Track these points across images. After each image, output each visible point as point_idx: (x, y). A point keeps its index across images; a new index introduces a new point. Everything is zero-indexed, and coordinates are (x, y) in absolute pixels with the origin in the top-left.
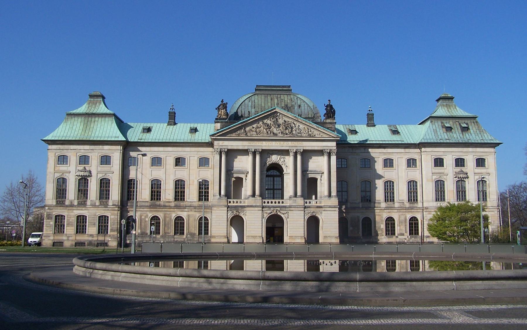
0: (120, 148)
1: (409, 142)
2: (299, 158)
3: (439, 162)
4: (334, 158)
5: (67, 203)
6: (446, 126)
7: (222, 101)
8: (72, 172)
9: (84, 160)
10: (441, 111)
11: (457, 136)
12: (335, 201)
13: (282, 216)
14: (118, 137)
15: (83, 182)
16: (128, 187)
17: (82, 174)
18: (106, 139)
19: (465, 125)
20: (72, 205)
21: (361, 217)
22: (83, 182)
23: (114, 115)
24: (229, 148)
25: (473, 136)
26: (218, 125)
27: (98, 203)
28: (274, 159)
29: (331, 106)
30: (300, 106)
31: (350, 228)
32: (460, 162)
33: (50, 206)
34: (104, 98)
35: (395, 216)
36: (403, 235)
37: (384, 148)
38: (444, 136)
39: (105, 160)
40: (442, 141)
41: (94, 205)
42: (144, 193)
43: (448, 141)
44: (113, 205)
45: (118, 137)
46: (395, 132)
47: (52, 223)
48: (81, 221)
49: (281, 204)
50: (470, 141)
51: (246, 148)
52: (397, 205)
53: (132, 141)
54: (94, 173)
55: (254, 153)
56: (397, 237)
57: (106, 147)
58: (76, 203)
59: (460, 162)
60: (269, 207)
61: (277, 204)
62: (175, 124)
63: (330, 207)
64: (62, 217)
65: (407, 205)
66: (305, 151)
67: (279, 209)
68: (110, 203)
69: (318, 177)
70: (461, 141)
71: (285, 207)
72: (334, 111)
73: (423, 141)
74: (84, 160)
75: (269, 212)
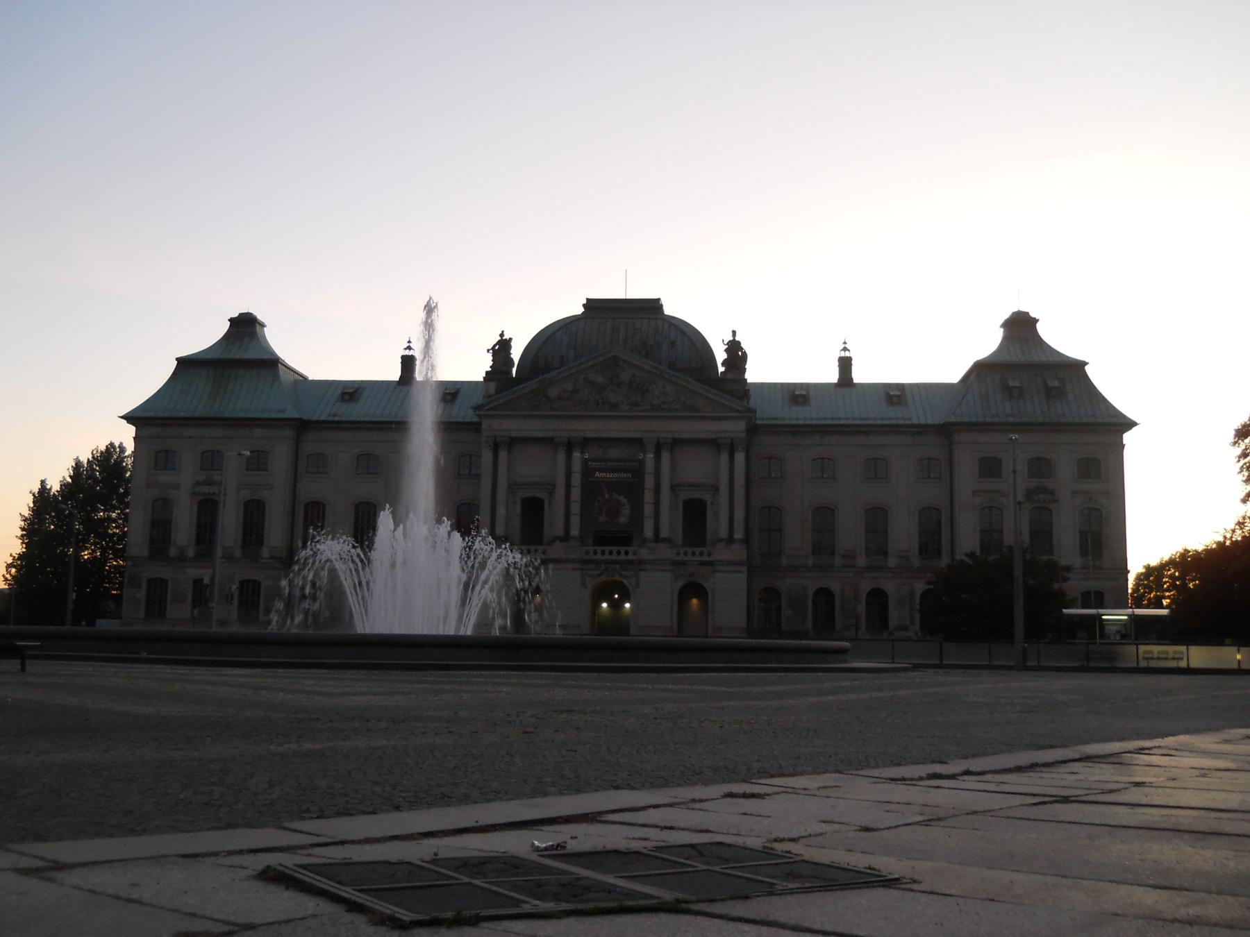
0: (289, 433)
1: (923, 421)
4: (740, 457)
5: (173, 552)
6: (1011, 383)
7: (502, 335)
9: (211, 460)
13: (625, 581)
14: (284, 411)
15: (208, 508)
17: (206, 489)
18: (257, 415)
19: (1056, 383)
20: (182, 559)
21: (812, 587)
22: (208, 508)
24: (514, 434)
26: (492, 385)
27: (238, 553)
29: (739, 343)
30: (673, 344)
31: (786, 612)
35: (890, 586)
36: (905, 628)
37: (866, 433)
39: (258, 462)
40: (996, 420)
41: (228, 557)
43: (1011, 420)
44: (272, 557)
45: (284, 411)
47: (142, 595)
48: (200, 593)
49: (622, 557)
50: (1062, 420)
51: (550, 434)
52: (892, 562)
53: (315, 418)
55: (569, 446)
56: (891, 634)
57: (258, 432)
58: (191, 553)
60: (597, 563)
61: (615, 557)
63: (729, 563)
64: (164, 582)
65: (916, 563)
67: (617, 567)
68: (265, 552)
69: (707, 497)
70: (1040, 420)
71: (631, 562)
72: (745, 356)
73: (953, 419)
74: (211, 460)
75: (596, 572)
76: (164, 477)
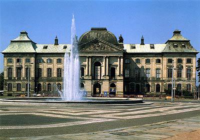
0: (34, 55)
2: (107, 59)
3: (170, 61)
4: (122, 60)
8: (14, 65)
10: (174, 39)
11: (179, 50)
12: (122, 78)
16: (38, 71)
23: (31, 41)
25: (186, 50)
28: (98, 60)
32: (180, 61)
33: (6, 80)
34: (27, 33)
38: (173, 50)
39: (28, 61)
42: (45, 74)
46: (153, 48)
54: (23, 66)
59: (180, 61)
62: (58, 44)
66: (109, 57)
76: (11, 64)
